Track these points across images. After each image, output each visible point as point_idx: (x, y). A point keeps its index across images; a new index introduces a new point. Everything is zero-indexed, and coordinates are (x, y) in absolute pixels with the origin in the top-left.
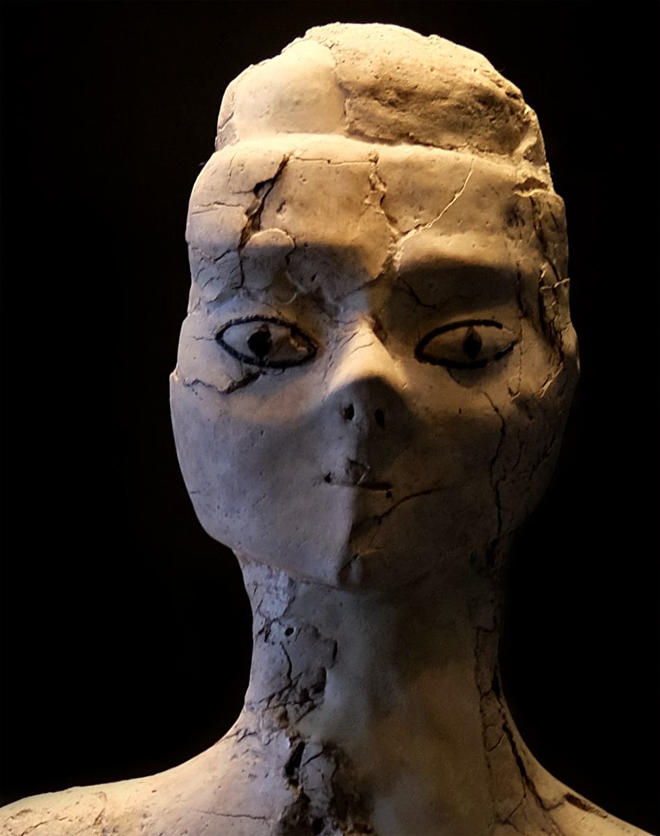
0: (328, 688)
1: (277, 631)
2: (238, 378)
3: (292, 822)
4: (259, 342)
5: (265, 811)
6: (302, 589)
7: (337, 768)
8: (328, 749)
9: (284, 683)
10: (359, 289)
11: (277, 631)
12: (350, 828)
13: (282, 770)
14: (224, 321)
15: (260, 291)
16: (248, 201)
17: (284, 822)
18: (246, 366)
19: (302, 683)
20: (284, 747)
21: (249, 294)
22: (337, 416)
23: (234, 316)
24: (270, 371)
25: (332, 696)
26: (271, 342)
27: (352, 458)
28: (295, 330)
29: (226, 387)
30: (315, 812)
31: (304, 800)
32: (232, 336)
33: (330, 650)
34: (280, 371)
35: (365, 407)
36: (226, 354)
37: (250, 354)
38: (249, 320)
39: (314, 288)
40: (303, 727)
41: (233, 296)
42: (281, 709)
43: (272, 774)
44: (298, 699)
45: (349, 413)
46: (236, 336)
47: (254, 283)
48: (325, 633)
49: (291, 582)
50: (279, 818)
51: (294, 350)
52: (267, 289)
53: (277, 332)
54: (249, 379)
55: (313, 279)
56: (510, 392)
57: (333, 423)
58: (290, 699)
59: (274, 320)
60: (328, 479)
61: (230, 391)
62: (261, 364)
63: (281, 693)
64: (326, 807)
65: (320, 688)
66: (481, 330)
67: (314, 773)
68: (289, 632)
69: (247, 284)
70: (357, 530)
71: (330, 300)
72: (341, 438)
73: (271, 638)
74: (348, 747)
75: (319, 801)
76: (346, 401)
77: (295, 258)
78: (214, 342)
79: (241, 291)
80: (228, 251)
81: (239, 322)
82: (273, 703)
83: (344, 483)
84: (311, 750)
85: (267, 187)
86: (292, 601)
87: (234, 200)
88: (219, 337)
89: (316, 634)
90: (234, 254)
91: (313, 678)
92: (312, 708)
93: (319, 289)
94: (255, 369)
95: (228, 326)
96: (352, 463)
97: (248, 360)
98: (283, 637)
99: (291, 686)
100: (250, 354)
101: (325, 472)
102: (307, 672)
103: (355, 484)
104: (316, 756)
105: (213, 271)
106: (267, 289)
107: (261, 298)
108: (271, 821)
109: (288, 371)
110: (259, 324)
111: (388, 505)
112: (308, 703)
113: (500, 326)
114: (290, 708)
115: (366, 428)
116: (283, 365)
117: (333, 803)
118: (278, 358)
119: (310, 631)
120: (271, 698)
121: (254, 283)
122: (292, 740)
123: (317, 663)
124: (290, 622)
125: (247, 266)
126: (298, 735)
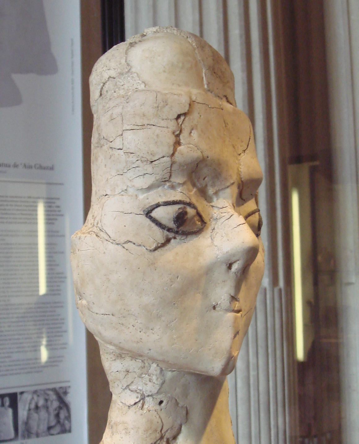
4: (180, 219)
6: (169, 375)
9: (158, 436)
10: (228, 187)
11: (150, 403)
14: (154, 203)
15: (179, 184)
16: (172, 125)
18: (166, 232)
19: (168, 435)
21: (173, 187)
22: (224, 267)
23: (162, 200)
24: (178, 237)
26: (187, 218)
27: (232, 294)
29: (153, 247)
32: (159, 213)
36: (153, 225)
37: (172, 225)
38: (174, 203)
41: (159, 187)
48: (181, 404)
51: (195, 224)
52: (184, 184)
53: (191, 212)
57: (220, 274)
61: (156, 249)
69: (173, 179)
71: (211, 191)
73: (146, 406)
78: (144, 217)
79: (168, 184)
80: (163, 157)
81: (167, 204)
85: (182, 118)
86: (163, 383)
87: (163, 123)
89: (177, 404)
93: (206, 186)
94: (171, 235)
95: (158, 205)
97: (169, 230)
98: (158, 407)
99: (162, 438)
100: (172, 225)
102: (172, 428)
105: (149, 168)
109: (189, 237)
110: (176, 207)
115: (239, 275)
116: (187, 234)
119: (174, 401)
121: (178, 179)
124: (160, 397)
125: (175, 167)
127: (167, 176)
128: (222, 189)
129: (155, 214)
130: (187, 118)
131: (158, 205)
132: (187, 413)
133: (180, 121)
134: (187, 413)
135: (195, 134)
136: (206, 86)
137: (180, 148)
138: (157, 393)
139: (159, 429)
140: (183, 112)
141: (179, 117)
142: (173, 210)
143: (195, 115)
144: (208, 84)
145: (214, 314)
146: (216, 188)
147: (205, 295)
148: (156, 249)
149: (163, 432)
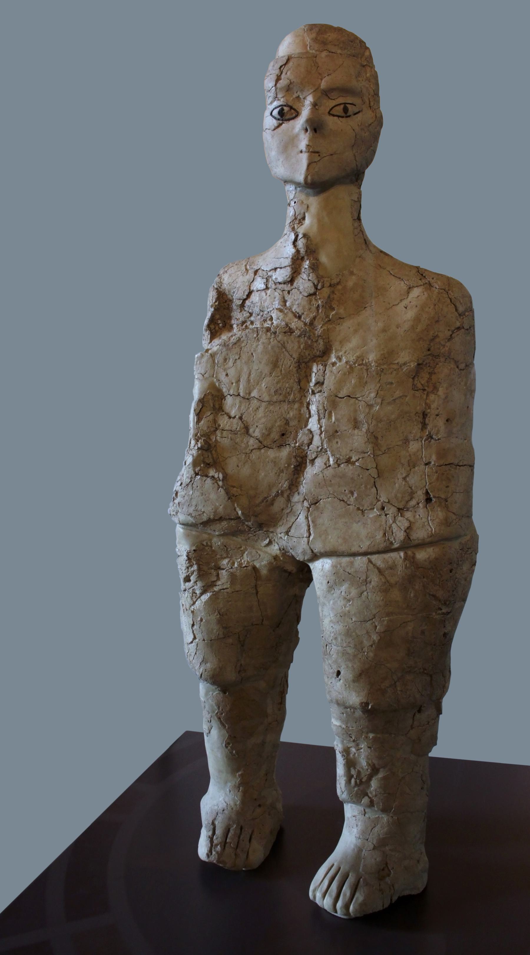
0: (306, 218)
1: (292, 203)
2: (276, 125)
3: (295, 258)
4: (281, 113)
5: (287, 256)
7: (307, 241)
8: (305, 236)
9: (294, 218)
10: (310, 94)
11: (292, 203)
12: (312, 259)
13: (292, 243)
16: (277, 72)
17: (292, 258)
18: (279, 121)
19: (299, 218)
20: (293, 237)
21: (279, 100)
22: (303, 132)
24: (285, 122)
25: (307, 221)
27: (307, 144)
28: (291, 108)
30: (302, 255)
31: (298, 251)
33: (306, 207)
34: (288, 122)
35: (310, 127)
36: (273, 119)
37: (279, 117)
38: (278, 107)
39: (297, 96)
40: (298, 230)
42: (293, 226)
43: (289, 245)
44: (297, 222)
45: (306, 130)
46: (275, 113)
47: (280, 96)
48: (305, 202)
49: (296, 188)
50: (291, 257)
52: (283, 97)
53: (286, 109)
54: (279, 125)
55: (297, 92)
56: (358, 125)
58: (296, 223)
59: (285, 106)
60: (301, 152)
61: (274, 130)
62: (282, 120)
63: (293, 221)
64: (304, 253)
65: (304, 218)
66: (348, 105)
67: (301, 243)
68: (295, 202)
69: (278, 96)
70: (309, 165)
72: (304, 139)
74: (311, 235)
75: (302, 251)
76: (305, 127)
77: (291, 86)
78: (270, 116)
79: (276, 99)
81: (276, 108)
82: (291, 224)
83: (305, 152)
84: (300, 236)
85: (283, 67)
86: (295, 194)
88: (271, 114)
89: (302, 202)
90: (274, 88)
91: (301, 216)
92: (302, 225)
94: (281, 122)
95: (274, 109)
96: (308, 146)
97: (279, 120)
99: (296, 219)
101: (300, 150)
102: (300, 214)
103: (308, 152)
104: (301, 238)
106: (283, 97)
107: (282, 100)
108: (289, 259)
111: (319, 158)
112: (301, 224)
113: (355, 105)
114: (296, 226)
115: (311, 134)
116: (289, 120)
117: (306, 251)
118: (287, 117)
119: (301, 202)
120: (290, 223)
122: (295, 234)
123: (302, 211)
124: (295, 200)
125: (278, 90)
126: (297, 232)
127: (275, 95)
128: (307, 96)
129: (274, 113)
130: (286, 66)
131: (274, 109)
132: (308, 207)
133: (282, 69)
134: (308, 207)
135: (289, 73)
136: (308, 48)
137: (281, 81)
138: (294, 198)
139: (294, 215)
140: (282, 64)
141: (281, 67)
142: (277, 110)
143: (291, 64)
144: (310, 46)
145: (301, 155)
146: (304, 96)
147: (297, 147)
148: (274, 130)
149: (296, 216)
